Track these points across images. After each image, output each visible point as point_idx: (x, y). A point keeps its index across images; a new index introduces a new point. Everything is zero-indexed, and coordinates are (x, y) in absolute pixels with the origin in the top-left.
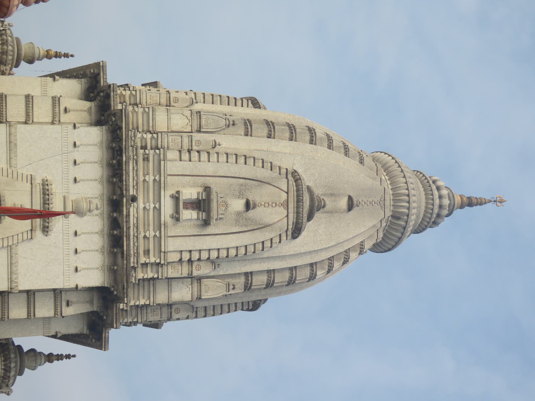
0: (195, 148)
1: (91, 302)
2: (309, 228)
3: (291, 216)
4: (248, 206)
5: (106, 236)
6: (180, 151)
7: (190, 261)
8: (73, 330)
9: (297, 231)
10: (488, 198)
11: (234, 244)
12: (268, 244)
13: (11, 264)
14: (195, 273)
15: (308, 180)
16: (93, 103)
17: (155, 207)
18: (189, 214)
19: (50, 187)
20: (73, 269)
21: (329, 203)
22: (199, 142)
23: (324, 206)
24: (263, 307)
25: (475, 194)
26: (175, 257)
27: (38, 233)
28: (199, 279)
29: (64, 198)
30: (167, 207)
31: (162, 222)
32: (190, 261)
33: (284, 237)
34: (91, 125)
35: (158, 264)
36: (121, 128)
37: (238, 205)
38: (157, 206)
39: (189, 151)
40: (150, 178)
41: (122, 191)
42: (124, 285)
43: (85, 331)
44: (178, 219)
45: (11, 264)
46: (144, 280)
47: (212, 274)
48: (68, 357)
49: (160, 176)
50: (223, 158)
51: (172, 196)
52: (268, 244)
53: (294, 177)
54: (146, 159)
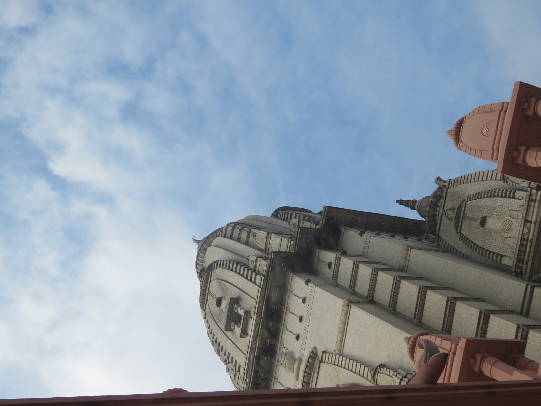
1: (319, 260)
4: (219, 302)
5: (283, 323)
13: (343, 333)
27: (320, 355)
29: (298, 379)
41: (258, 364)
42: (271, 270)
43: (343, 229)
45: (343, 333)
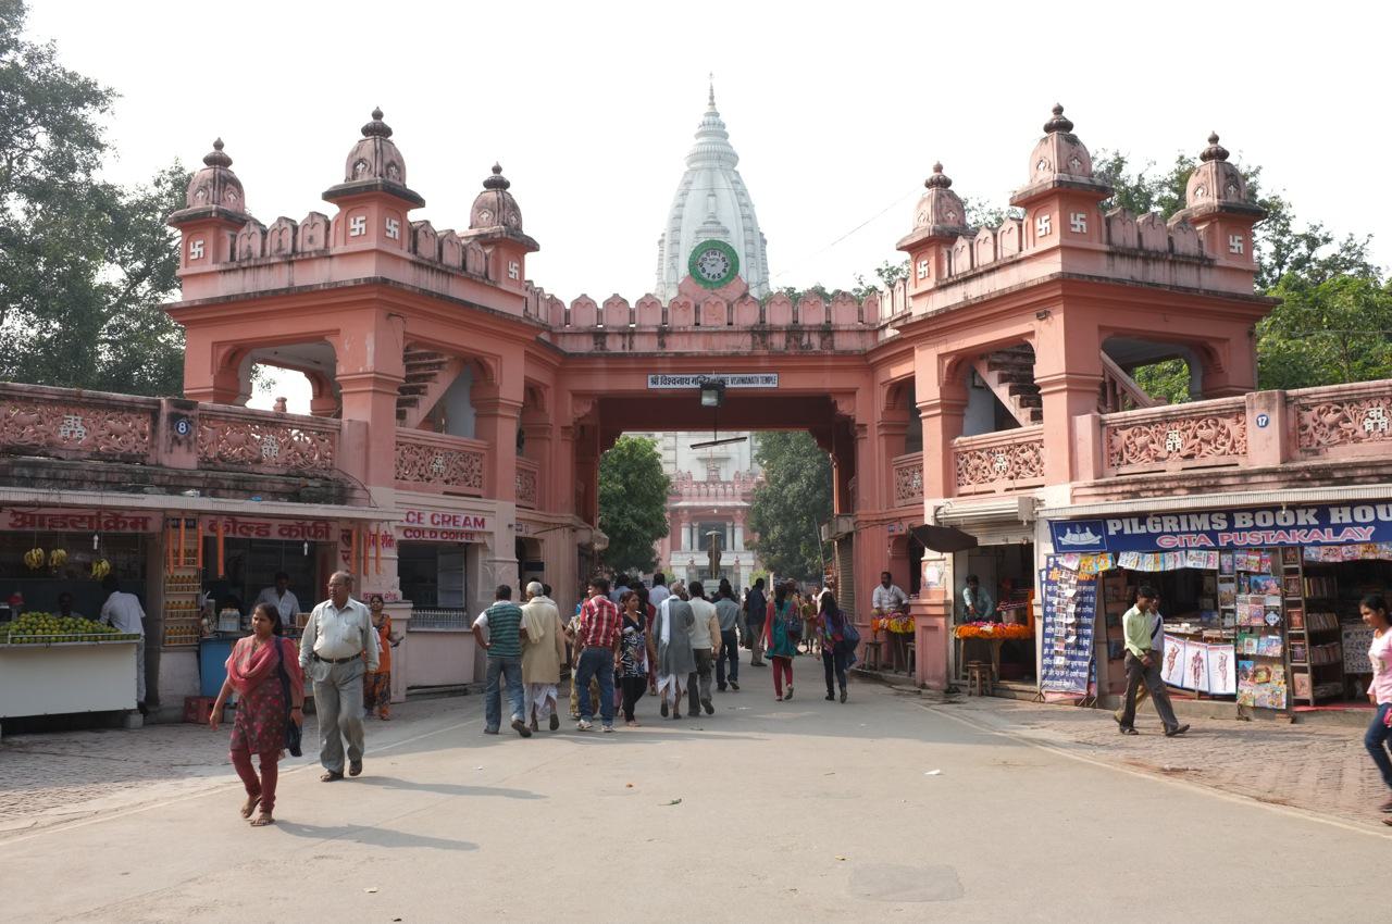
15: (699, 225)
21: (712, 210)
24: (765, 237)
25: (709, 94)
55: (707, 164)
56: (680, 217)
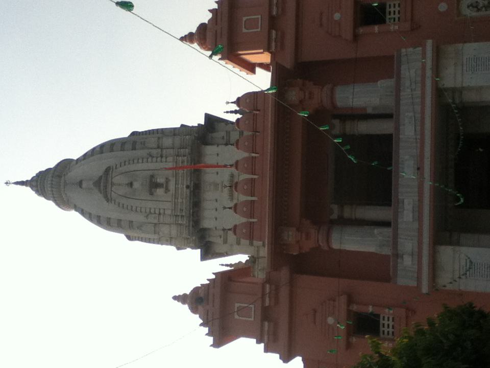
0: (157, 215)
1: (212, 137)
2: (101, 173)
3: (110, 179)
4: (131, 184)
6: (164, 213)
7: (162, 157)
8: (223, 124)
9: (108, 171)
10: (13, 185)
11: (140, 165)
12: (123, 164)
14: (160, 150)
16: (207, 239)
17: (178, 185)
18: (160, 180)
19: (229, 197)
20: (220, 155)
22: (155, 218)
23: (94, 183)
25: (19, 186)
26: (170, 159)
28: (158, 147)
30: (172, 186)
31: (175, 178)
32: (162, 157)
33: (114, 167)
34: (209, 229)
35: (178, 156)
36: (193, 226)
37: (136, 185)
38: (177, 186)
39: (160, 214)
40: (180, 200)
44: (167, 179)
46: (186, 148)
47: (150, 150)
48: (227, 112)
49: (175, 202)
50: (143, 210)
51: (169, 191)
52: (123, 164)
53: (108, 199)
54: (181, 210)
55: (62, 187)
56: (99, 217)
